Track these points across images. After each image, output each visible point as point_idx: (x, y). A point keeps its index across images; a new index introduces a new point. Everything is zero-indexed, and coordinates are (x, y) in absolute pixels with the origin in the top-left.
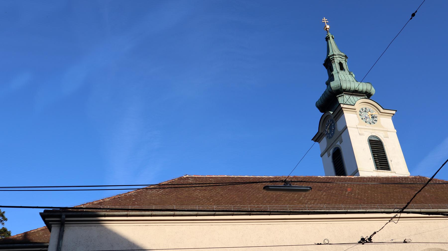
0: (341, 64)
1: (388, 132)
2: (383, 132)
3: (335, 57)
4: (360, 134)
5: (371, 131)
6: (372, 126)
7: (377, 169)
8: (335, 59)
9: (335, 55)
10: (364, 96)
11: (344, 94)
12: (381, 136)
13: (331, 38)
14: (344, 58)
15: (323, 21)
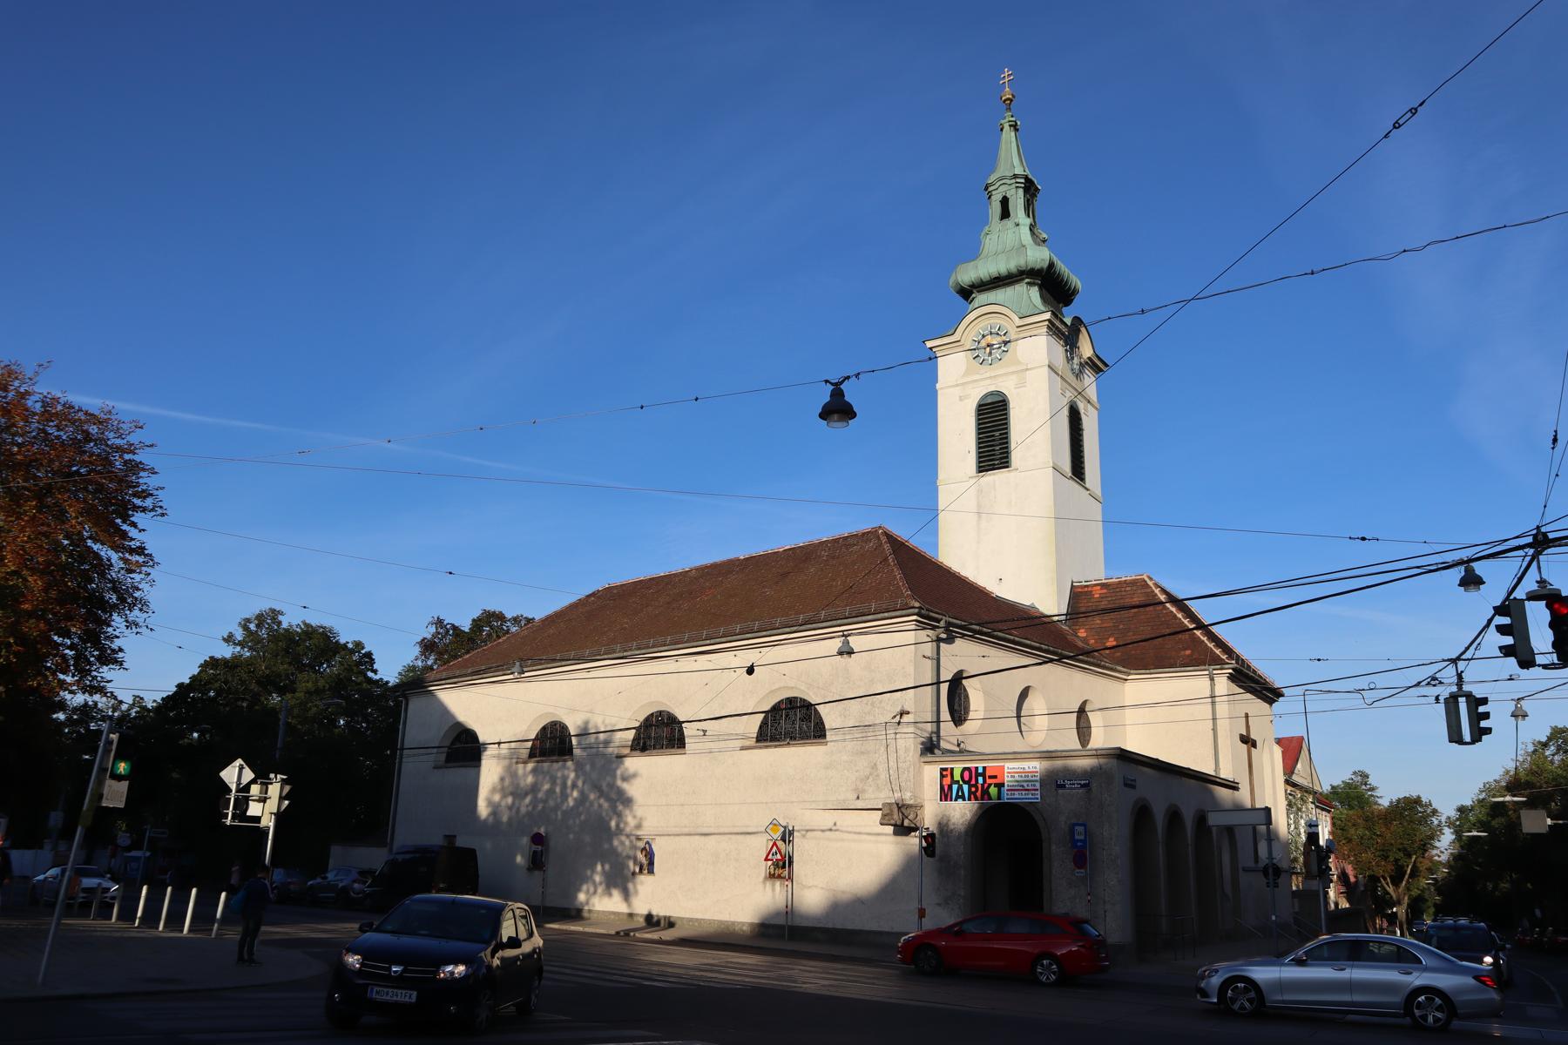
0: (1005, 202)
1: (1028, 372)
2: (1014, 377)
3: (990, 189)
4: (961, 399)
5: (988, 382)
6: (998, 369)
7: (980, 472)
8: (994, 193)
9: (992, 184)
10: (1023, 279)
11: (978, 292)
12: (1008, 387)
13: (1006, 127)
14: (1014, 181)
15: (1001, 82)
